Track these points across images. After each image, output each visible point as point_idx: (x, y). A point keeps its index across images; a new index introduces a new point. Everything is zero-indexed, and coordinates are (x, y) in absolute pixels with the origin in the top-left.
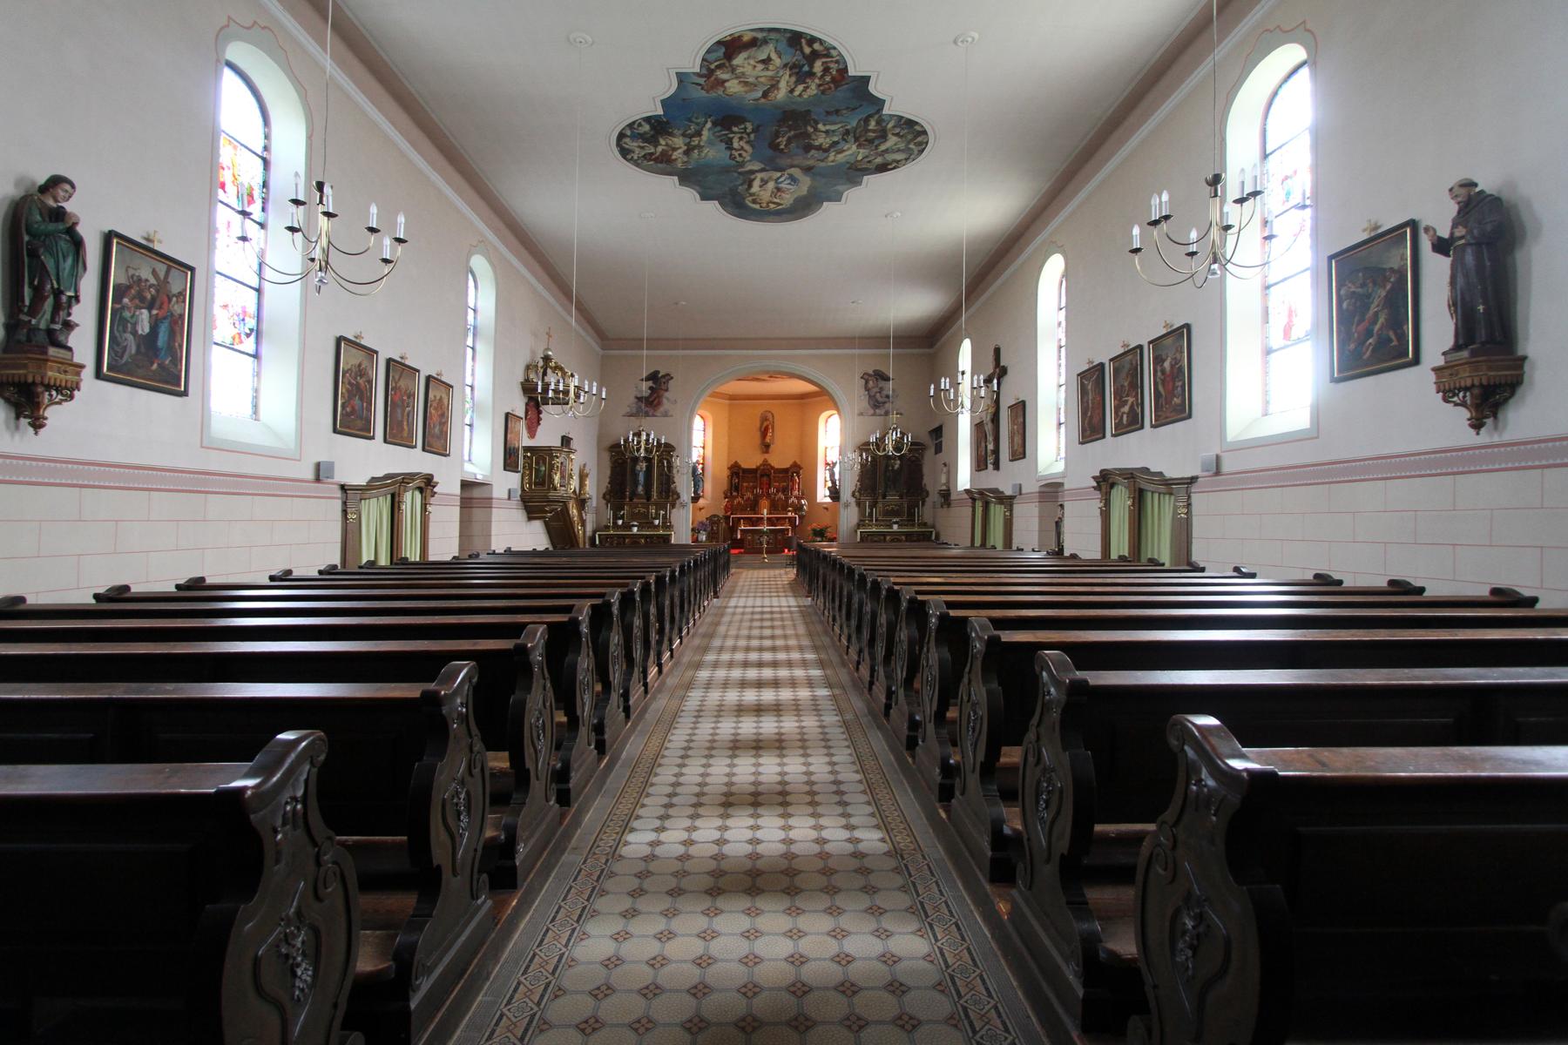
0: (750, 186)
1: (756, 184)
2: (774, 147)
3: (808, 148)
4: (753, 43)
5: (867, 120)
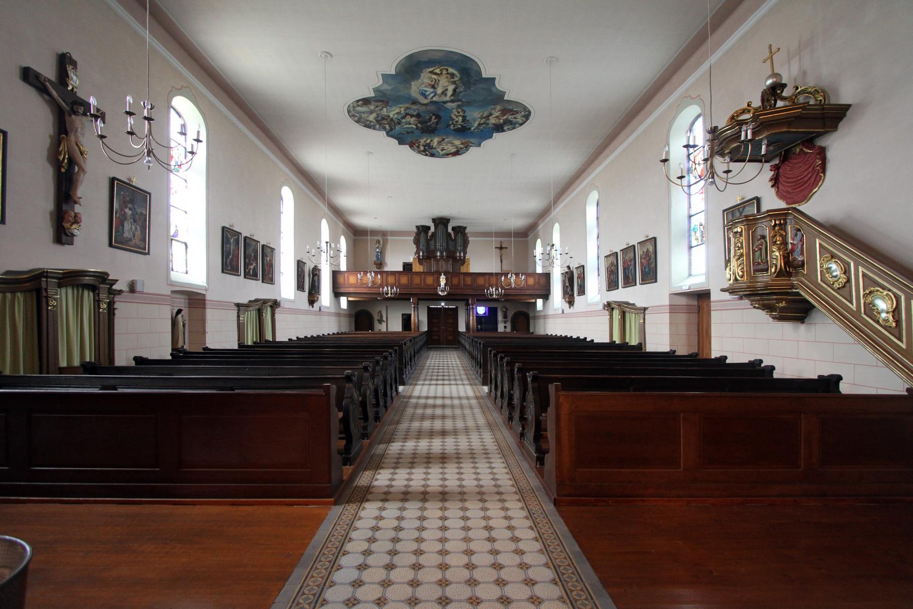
0: (455, 90)
1: (450, 93)
2: (438, 117)
3: (418, 116)
4: (448, 155)
5: (391, 130)
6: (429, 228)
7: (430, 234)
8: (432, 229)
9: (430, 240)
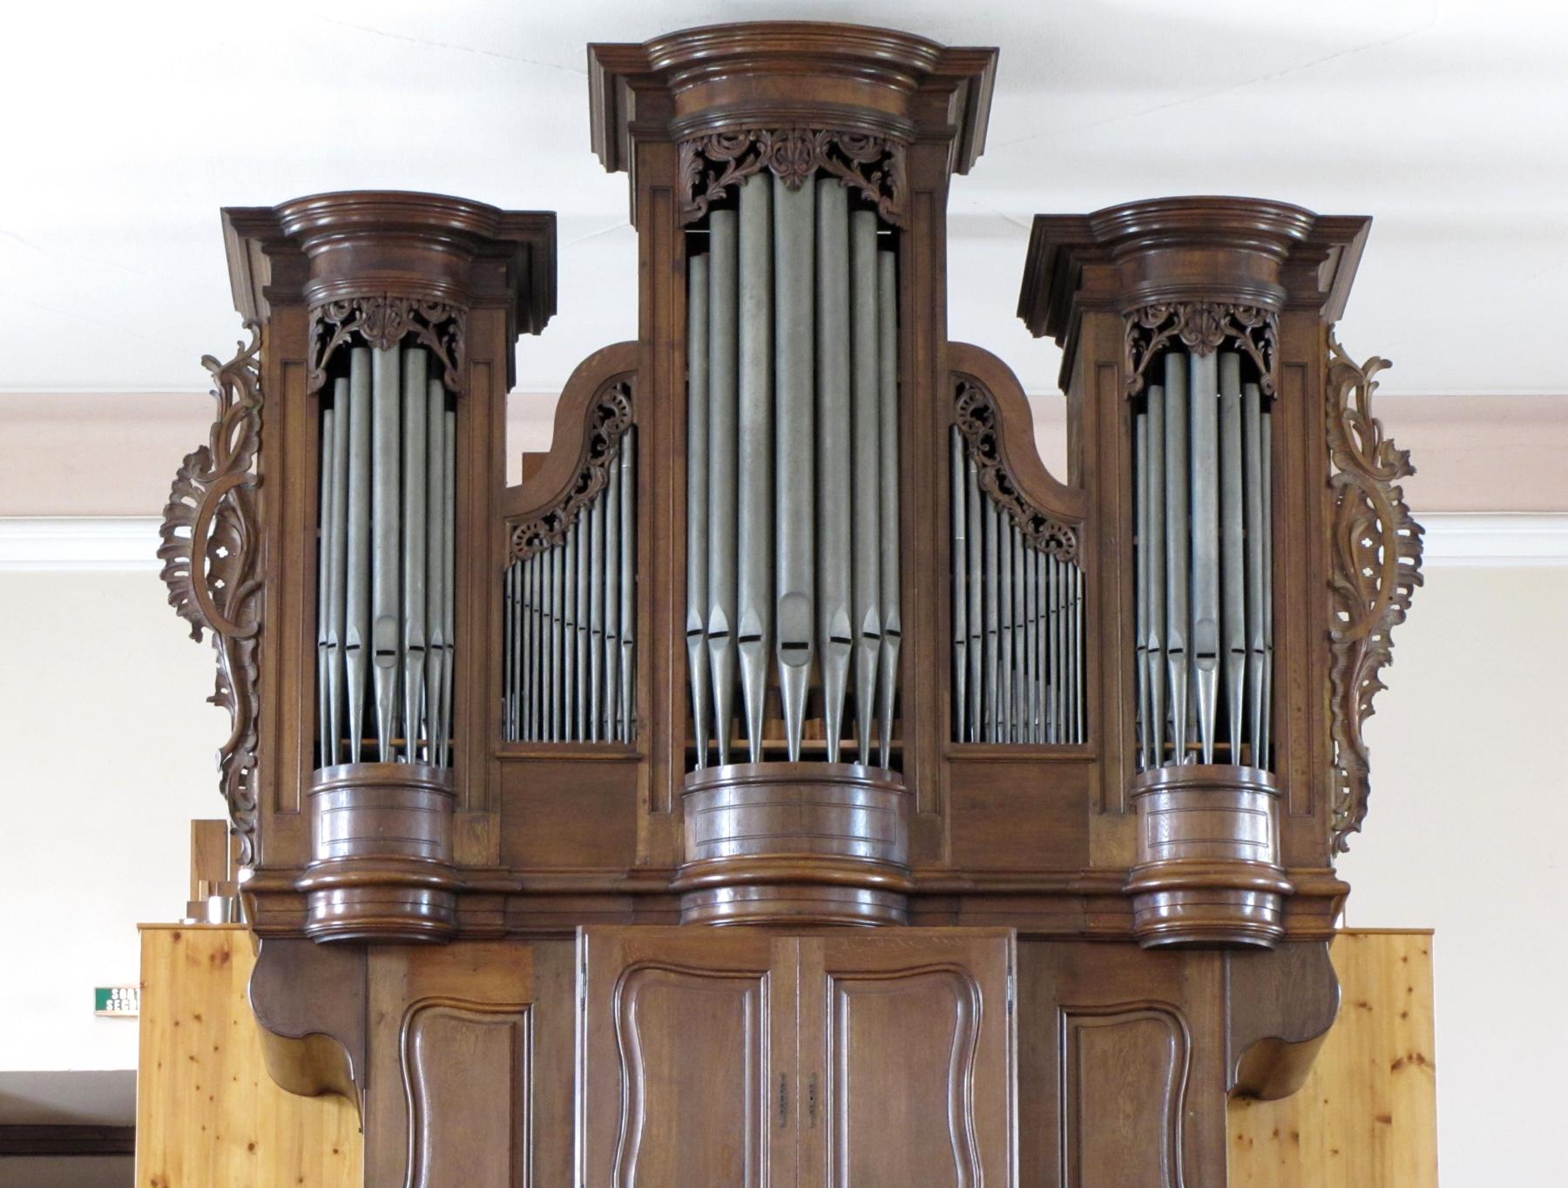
6: (511, 261)
7: (530, 424)
8: (599, 297)
9: (547, 521)
